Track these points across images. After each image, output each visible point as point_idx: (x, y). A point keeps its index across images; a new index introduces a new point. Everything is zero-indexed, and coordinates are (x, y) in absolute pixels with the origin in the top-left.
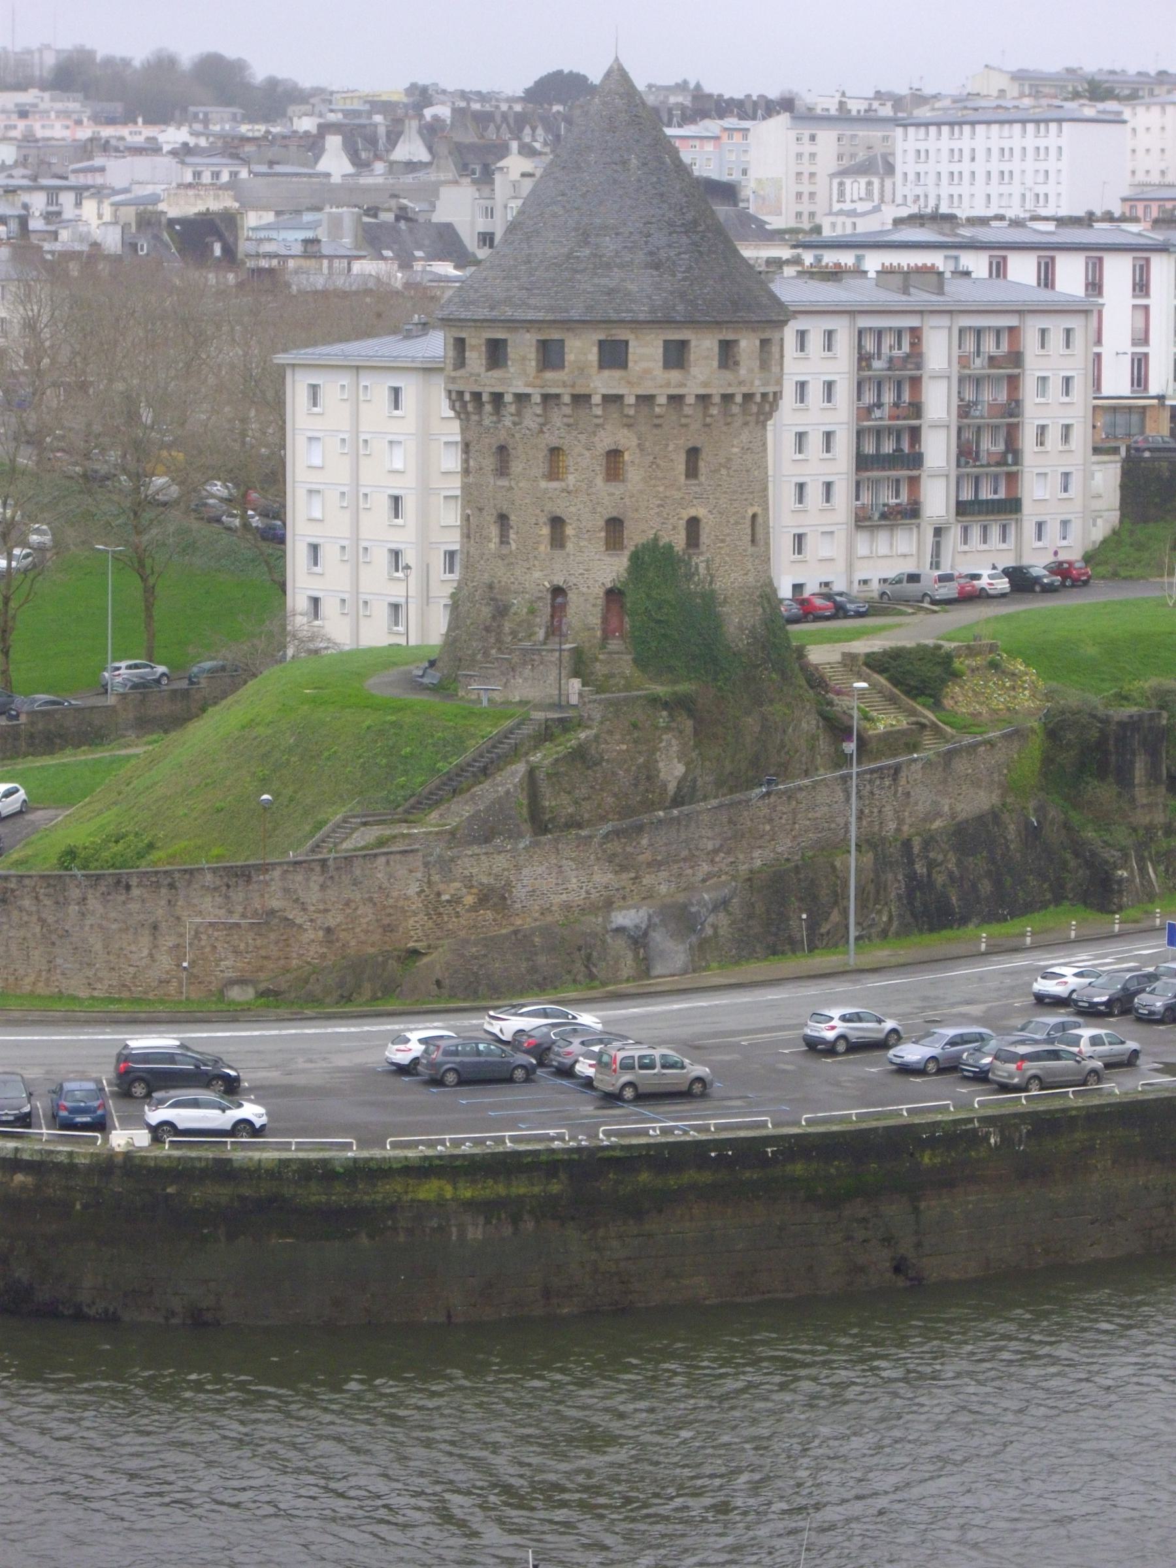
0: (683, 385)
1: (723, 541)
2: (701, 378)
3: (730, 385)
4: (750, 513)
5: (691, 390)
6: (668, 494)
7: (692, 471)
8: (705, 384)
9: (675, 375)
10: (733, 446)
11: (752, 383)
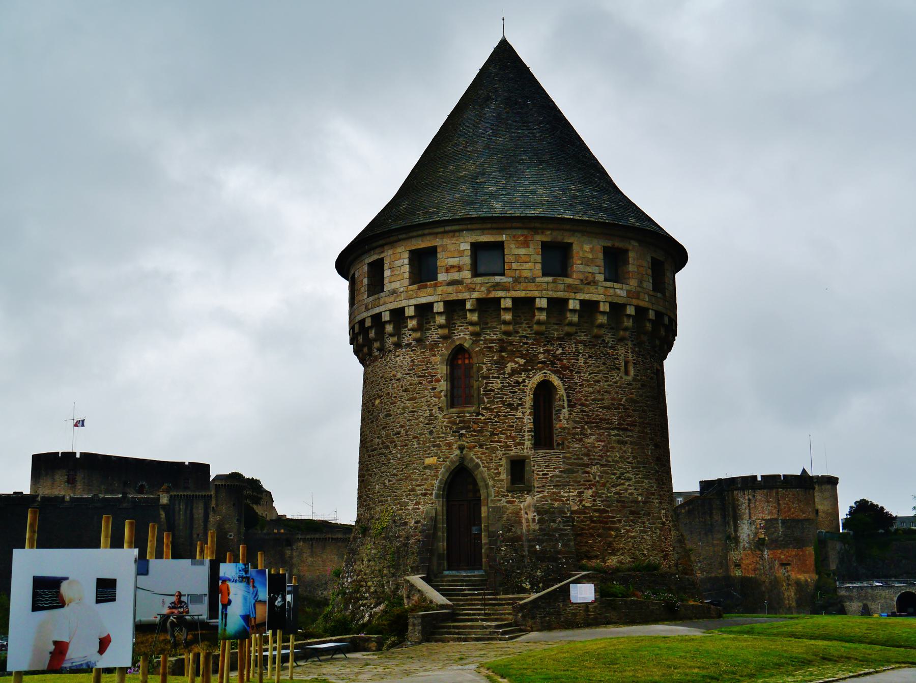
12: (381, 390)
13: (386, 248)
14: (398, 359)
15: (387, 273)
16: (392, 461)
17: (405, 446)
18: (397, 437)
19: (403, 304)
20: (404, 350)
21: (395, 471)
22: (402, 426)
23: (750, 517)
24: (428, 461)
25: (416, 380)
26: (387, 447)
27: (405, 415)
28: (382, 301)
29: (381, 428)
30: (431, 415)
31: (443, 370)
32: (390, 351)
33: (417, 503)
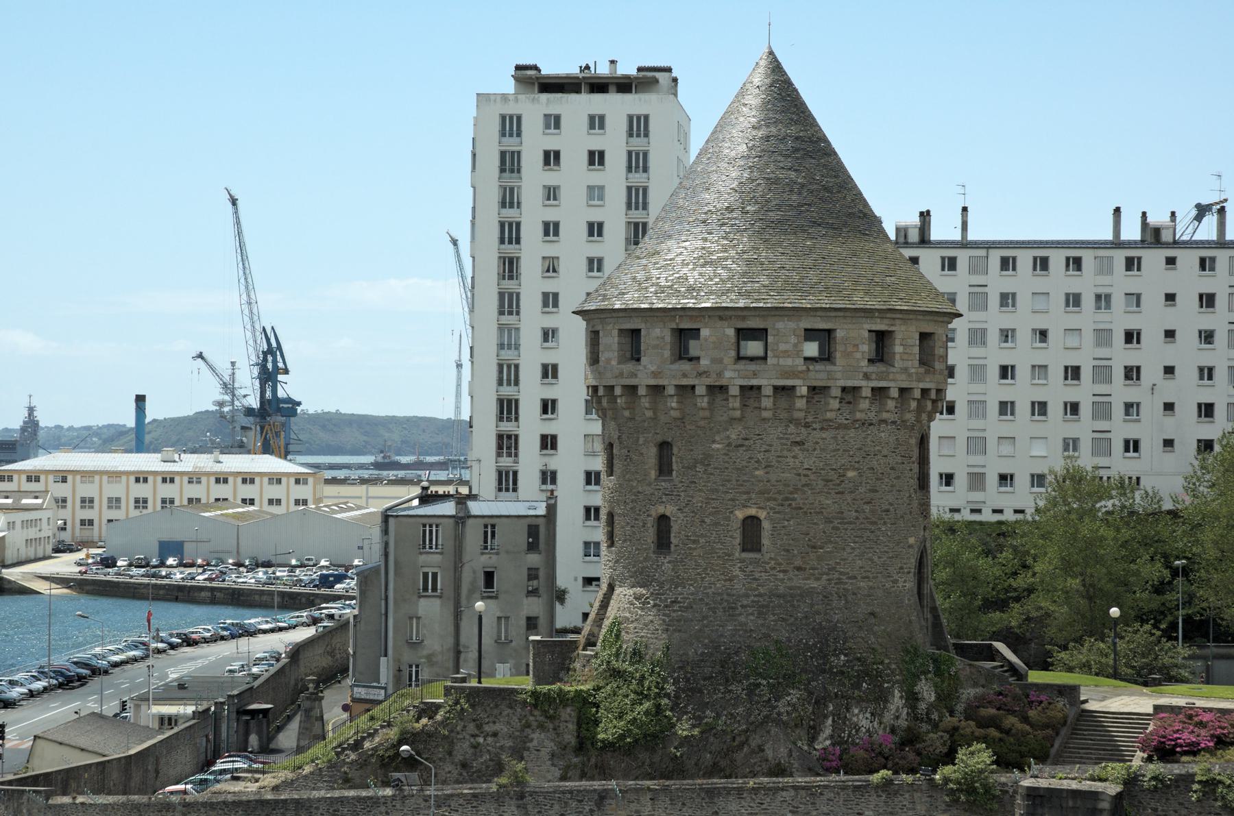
0: (634, 375)
1: (694, 542)
2: (653, 368)
3: (685, 375)
4: (740, 514)
6: (640, 489)
7: (664, 468)
8: (655, 375)
9: (629, 367)
10: (714, 442)
11: (720, 375)
12: (858, 462)
13: (898, 322)
14: (883, 434)
15: (898, 349)
16: (881, 538)
17: (895, 524)
18: (886, 515)
19: (913, 385)
20: (889, 427)
21: (886, 549)
22: (891, 504)
24: (912, 540)
25: (899, 459)
26: (875, 523)
27: (894, 493)
28: (891, 376)
29: (862, 502)
30: (910, 496)
31: (915, 453)
32: (871, 424)
33: (905, 581)
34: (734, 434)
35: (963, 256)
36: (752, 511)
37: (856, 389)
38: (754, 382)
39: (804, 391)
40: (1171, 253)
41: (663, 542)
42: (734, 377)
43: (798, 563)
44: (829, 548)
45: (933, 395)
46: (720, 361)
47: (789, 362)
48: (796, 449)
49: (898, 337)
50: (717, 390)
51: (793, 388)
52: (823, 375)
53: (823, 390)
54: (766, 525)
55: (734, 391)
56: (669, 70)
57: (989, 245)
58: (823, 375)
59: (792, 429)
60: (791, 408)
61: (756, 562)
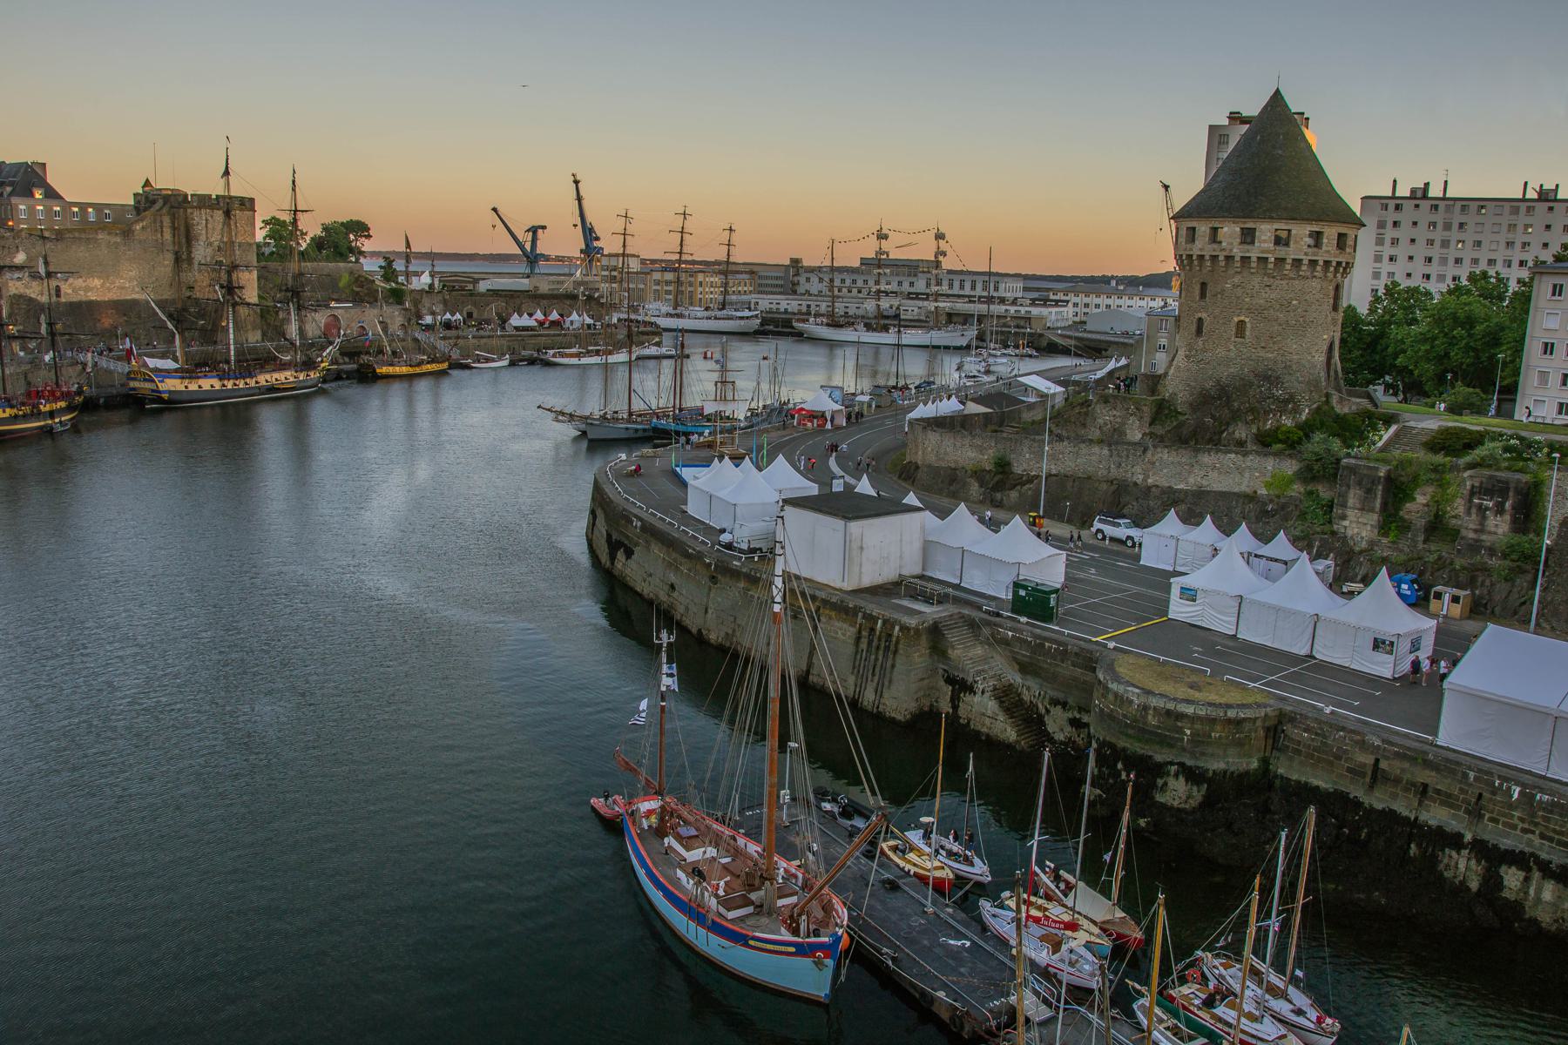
0: (1191, 250)
2: (1200, 246)
4: (1236, 319)
5: (1196, 252)
7: (1203, 295)
8: (1201, 250)
9: (1189, 246)
11: (1231, 250)
15: (1325, 241)
23: (207, 238)
24: (1325, 337)
31: (1332, 294)
34: (1236, 280)
35: (1442, 205)
36: (1242, 318)
37: (1300, 261)
38: (1247, 255)
39: (1273, 259)
40: (1552, 204)
41: (1199, 331)
42: (1238, 252)
43: (1263, 345)
44: (1279, 338)
45: (1344, 265)
46: (1232, 244)
47: (1266, 245)
48: (1267, 288)
49: (1325, 235)
50: (1229, 258)
51: (1267, 258)
52: (1283, 253)
53: (1283, 260)
54: (1248, 325)
55: (1238, 258)
56: (1303, 114)
57: (1455, 199)
58: (1283, 253)
59: (1266, 279)
60: (1266, 268)
61: (1242, 343)
